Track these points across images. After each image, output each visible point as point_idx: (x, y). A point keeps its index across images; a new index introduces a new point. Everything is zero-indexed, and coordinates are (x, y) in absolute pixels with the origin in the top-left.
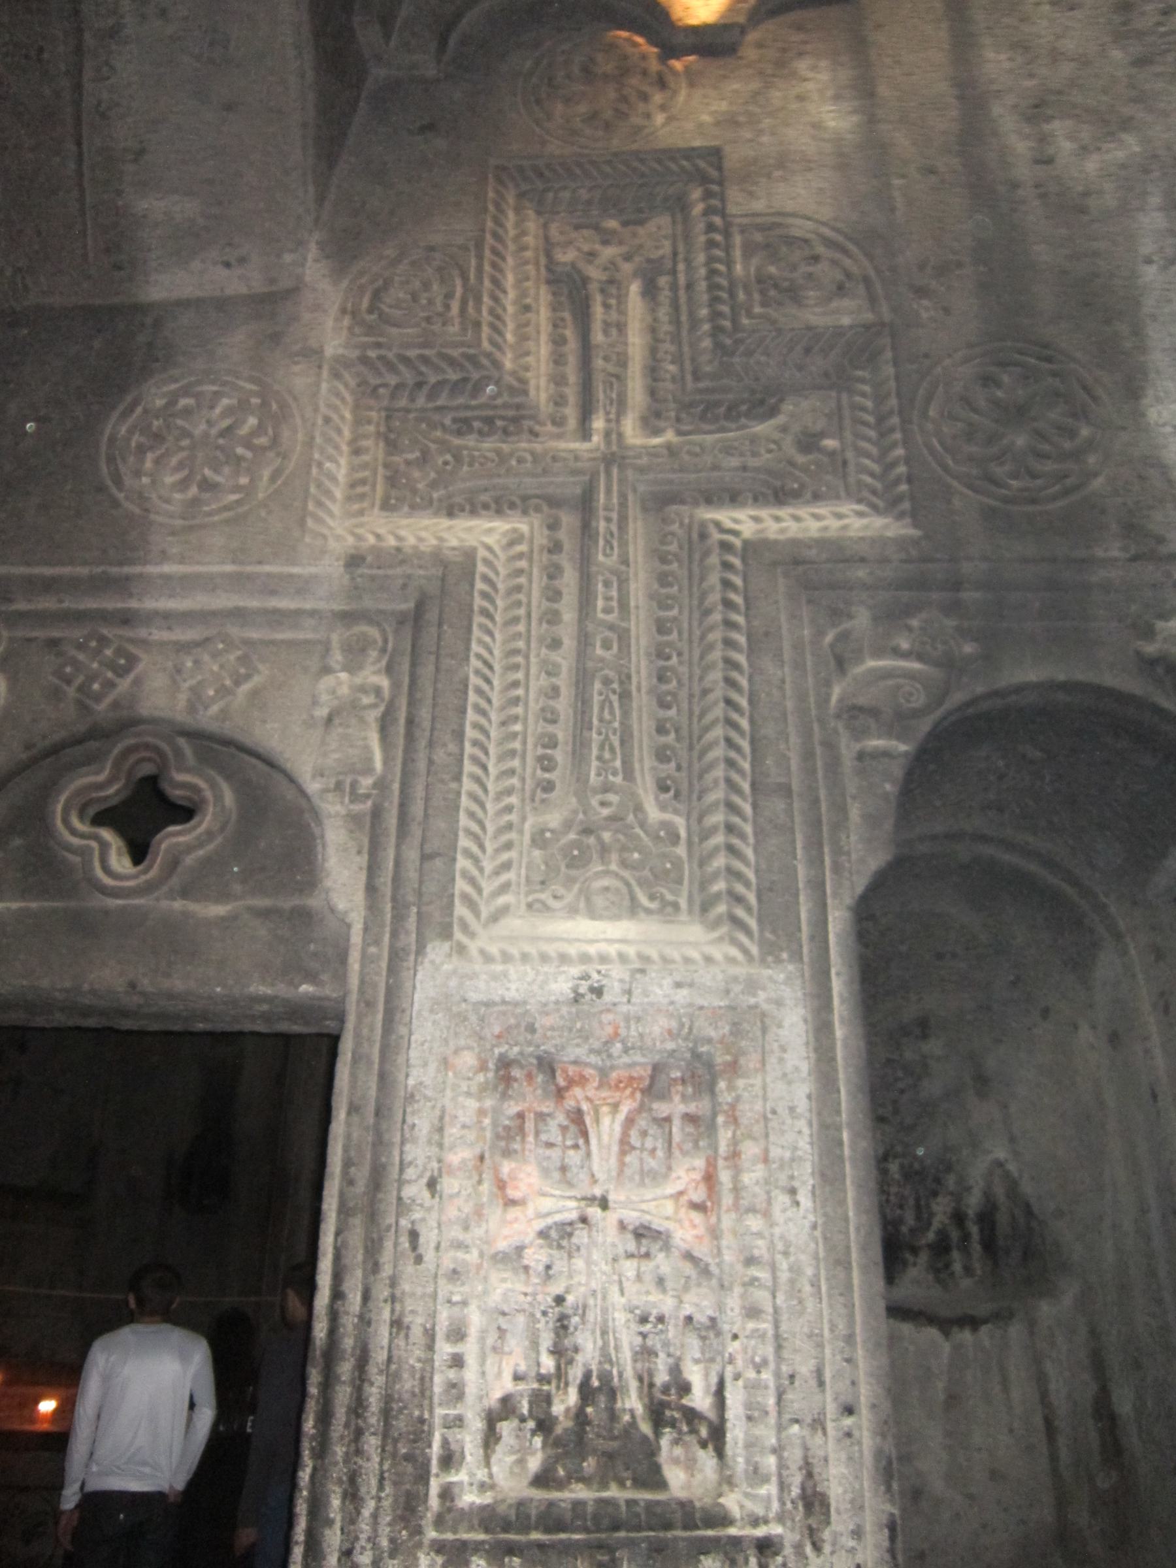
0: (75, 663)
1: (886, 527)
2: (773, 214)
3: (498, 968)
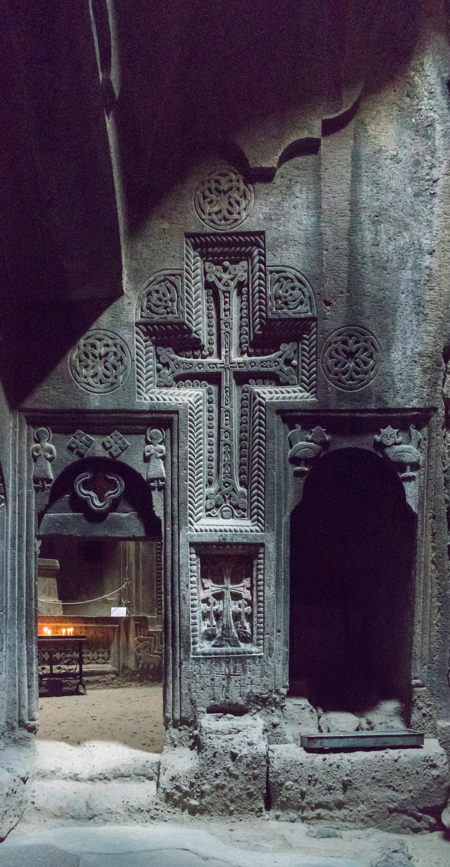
2: (283, 266)
3: (200, 533)
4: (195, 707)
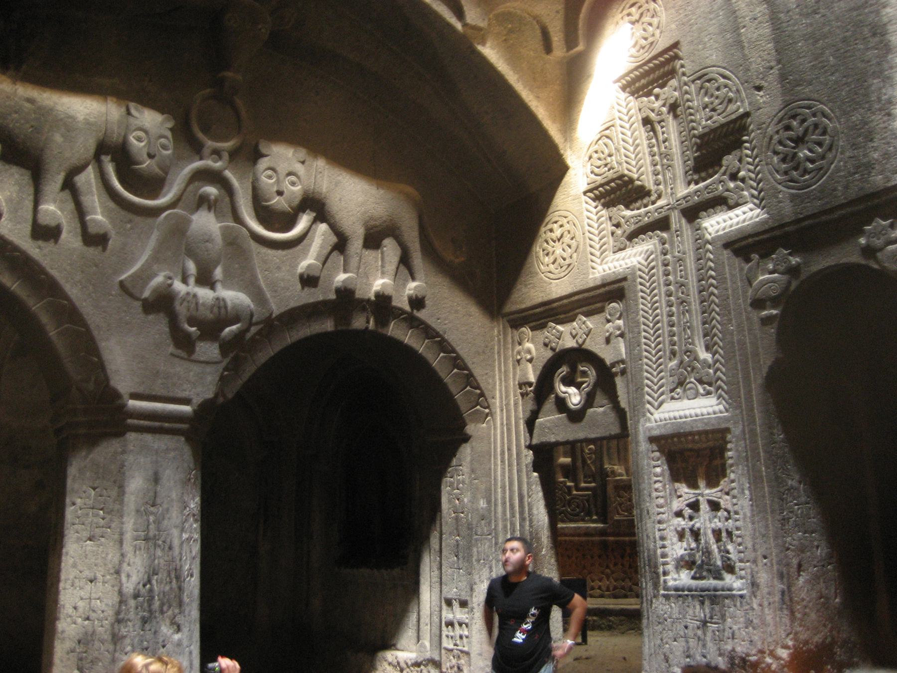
1: (758, 216)
4: (670, 666)
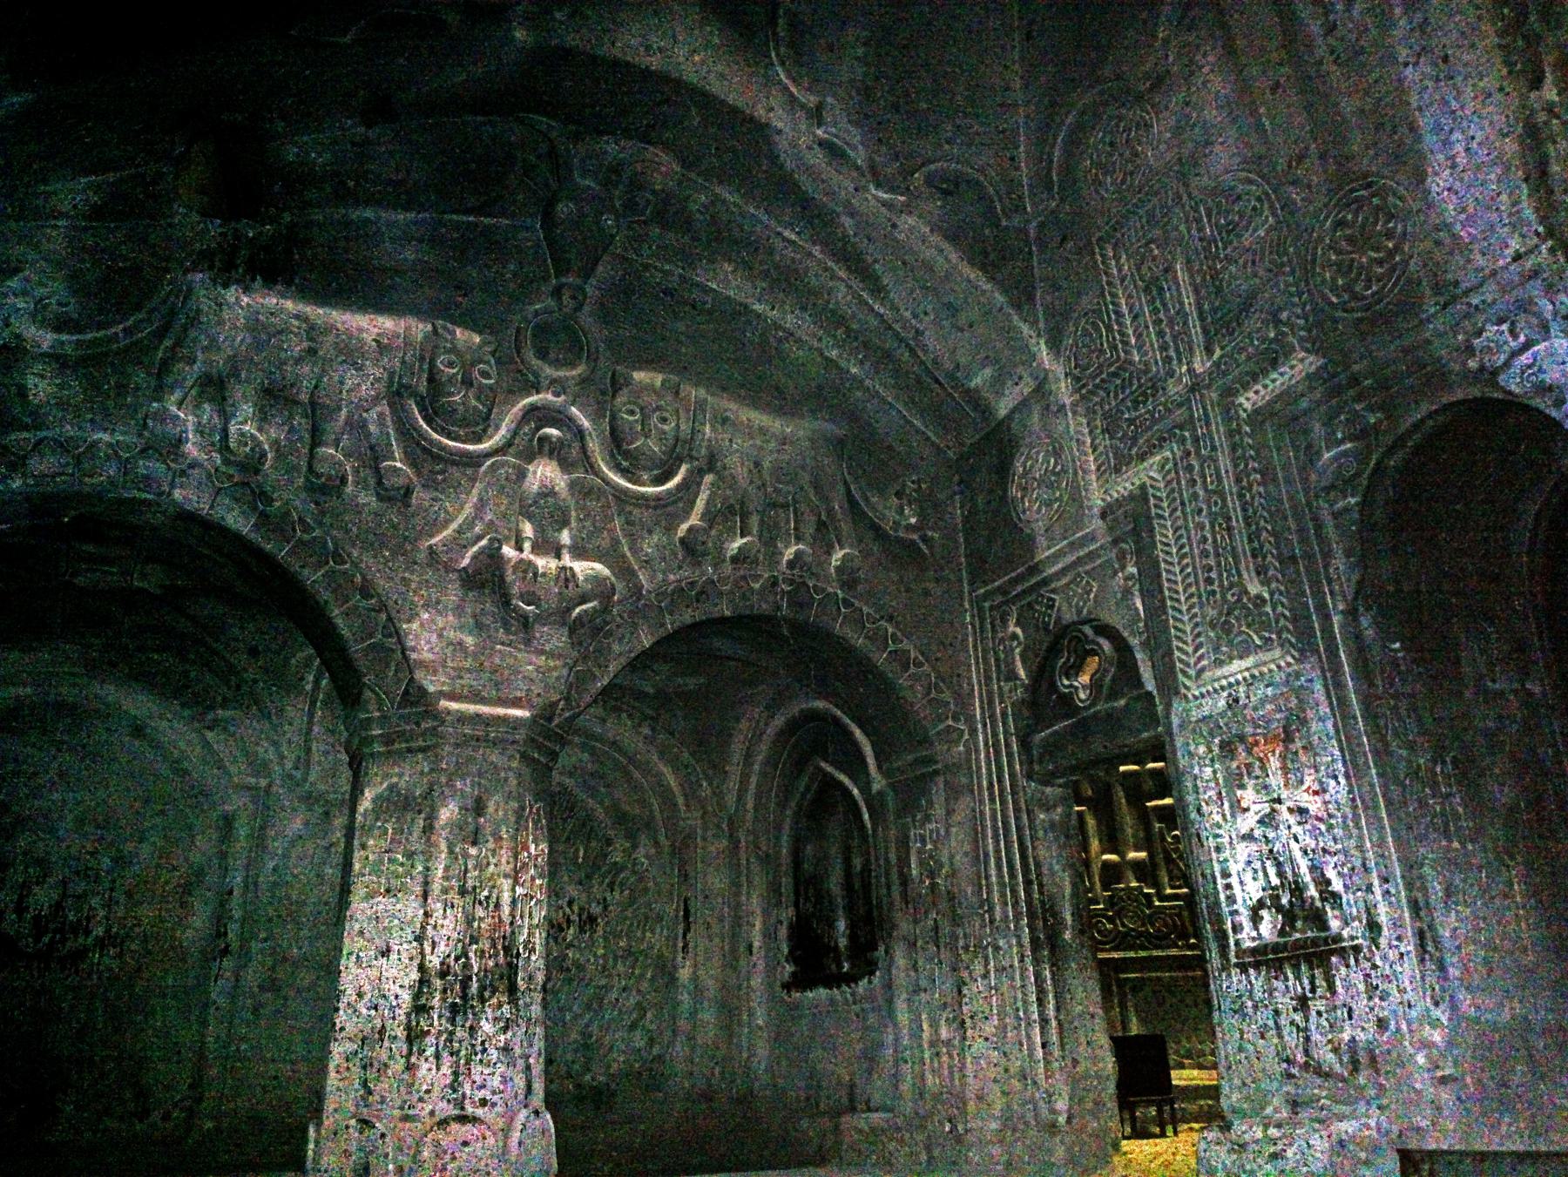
0: (1040, 613)
